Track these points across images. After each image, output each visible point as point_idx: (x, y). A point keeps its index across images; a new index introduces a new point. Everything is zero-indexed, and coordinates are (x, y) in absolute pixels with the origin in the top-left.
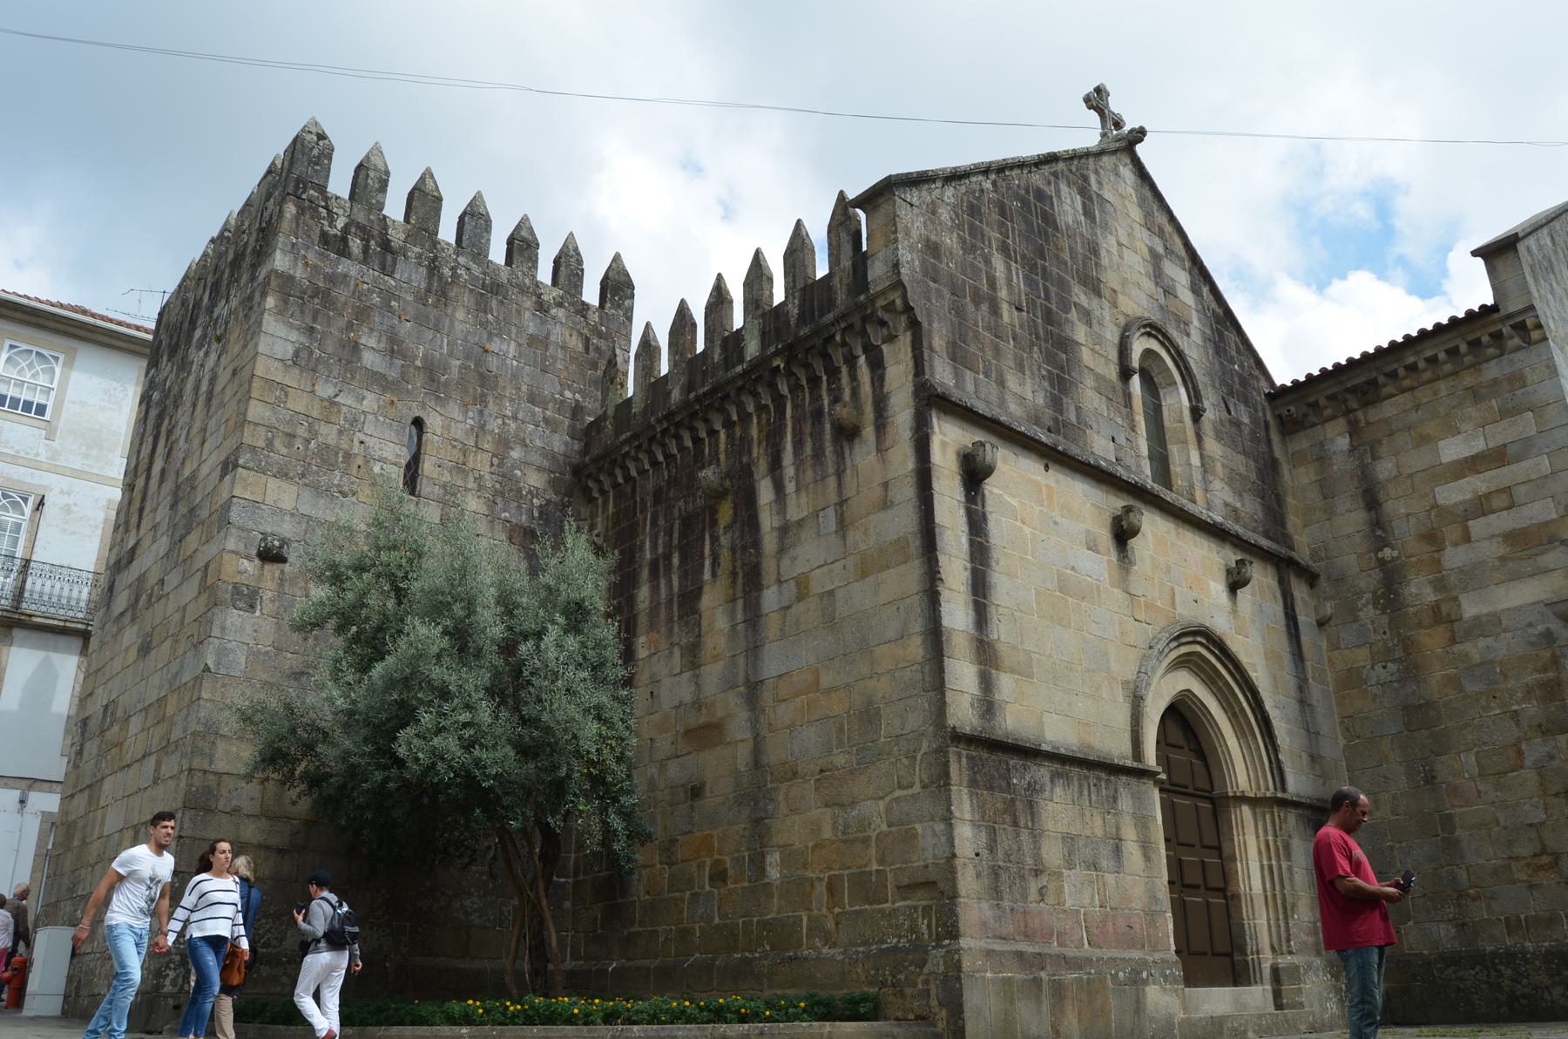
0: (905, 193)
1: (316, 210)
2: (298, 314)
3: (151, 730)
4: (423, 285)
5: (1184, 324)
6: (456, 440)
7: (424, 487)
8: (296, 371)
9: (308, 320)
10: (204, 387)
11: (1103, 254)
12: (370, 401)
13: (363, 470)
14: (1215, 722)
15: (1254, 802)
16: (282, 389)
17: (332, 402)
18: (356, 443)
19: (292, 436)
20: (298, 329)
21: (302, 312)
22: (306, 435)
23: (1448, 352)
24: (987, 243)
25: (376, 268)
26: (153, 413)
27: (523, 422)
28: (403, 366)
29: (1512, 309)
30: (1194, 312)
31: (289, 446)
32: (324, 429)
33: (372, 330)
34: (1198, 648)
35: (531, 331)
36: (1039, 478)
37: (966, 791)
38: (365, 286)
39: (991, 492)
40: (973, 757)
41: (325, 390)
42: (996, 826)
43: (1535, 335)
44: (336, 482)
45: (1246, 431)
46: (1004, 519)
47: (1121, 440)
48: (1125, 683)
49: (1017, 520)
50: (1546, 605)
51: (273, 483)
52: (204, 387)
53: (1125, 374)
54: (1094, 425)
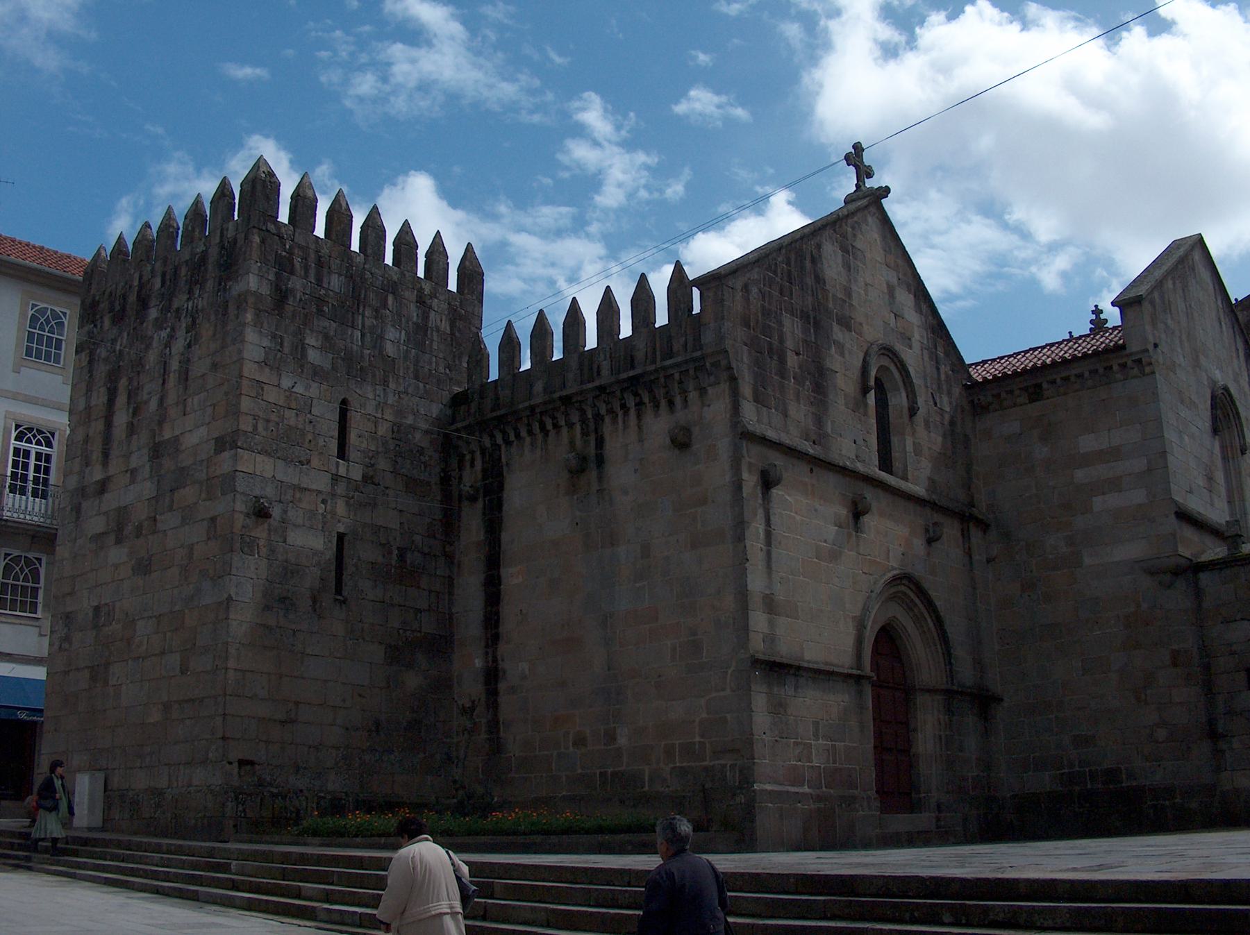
3: (169, 634)
5: (907, 340)
6: (369, 414)
7: (353, 454)
8: (267, 370)
10: (175, 365)
11: (854, 295)
13: (313, 443)
22: (277, 419)
23: (1091, 372)
26: (102, 370)
27: (412, 396)
29: (1134, 349)
30: (916, 328)
34: (903, 588)
35: (415, 319)
36: (807, 480)
43: (1147, 370)
45: (947, 417)
47: (860, 442)
48: (854, 618)
52: (175, 365)
53: (865, 390)
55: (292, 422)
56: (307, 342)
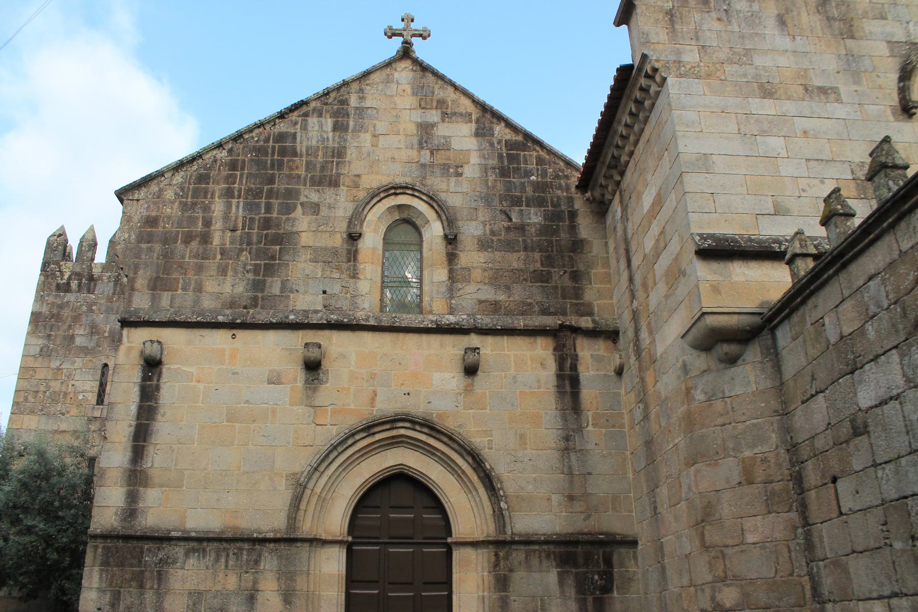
0: (133, 194)
1: (54, 274)
2: (43, 330)
4: (111, 291)
8: (40, 359)
9: (48, 332)
12: (79, 362)
13: (73, 399)
14: (437, 484)
15: (475, 544)
16: (33, 370)
17: (58, 369)
18: (70, 386)
19: (37, 392)
20: (42, 338)
21: (45, 328)
24: (209, 196)
25: (85, 292)
28: (98, 339)
31: (35, 397)
32: (53, 384)
33: (81, 325)
37: (97, 569)
38: (79, 304)
39: (169, 369)
40: (109, 548)
41: (55, 364)
42: (122, 590)
44: (59, 409)
46: (177, 385)
47: (336, 289)
49: (192, 381)
50: (682, 337)
51: (26, 418)
54: (302, 289)
55: (57, 389)
56: (76, 333)
